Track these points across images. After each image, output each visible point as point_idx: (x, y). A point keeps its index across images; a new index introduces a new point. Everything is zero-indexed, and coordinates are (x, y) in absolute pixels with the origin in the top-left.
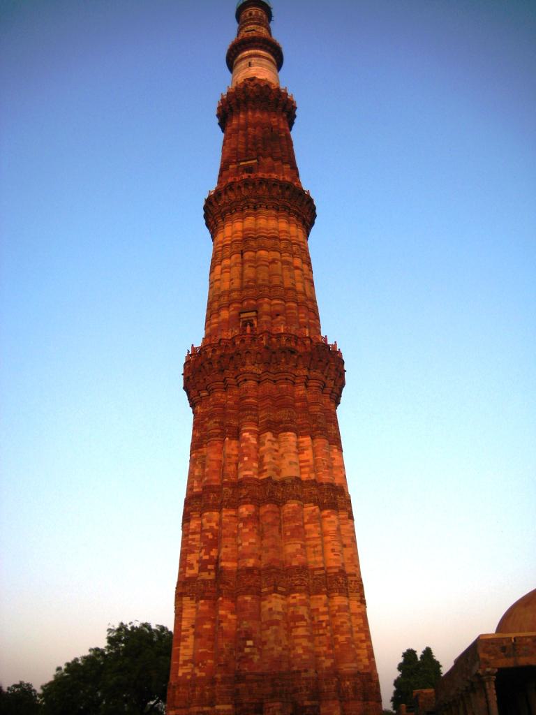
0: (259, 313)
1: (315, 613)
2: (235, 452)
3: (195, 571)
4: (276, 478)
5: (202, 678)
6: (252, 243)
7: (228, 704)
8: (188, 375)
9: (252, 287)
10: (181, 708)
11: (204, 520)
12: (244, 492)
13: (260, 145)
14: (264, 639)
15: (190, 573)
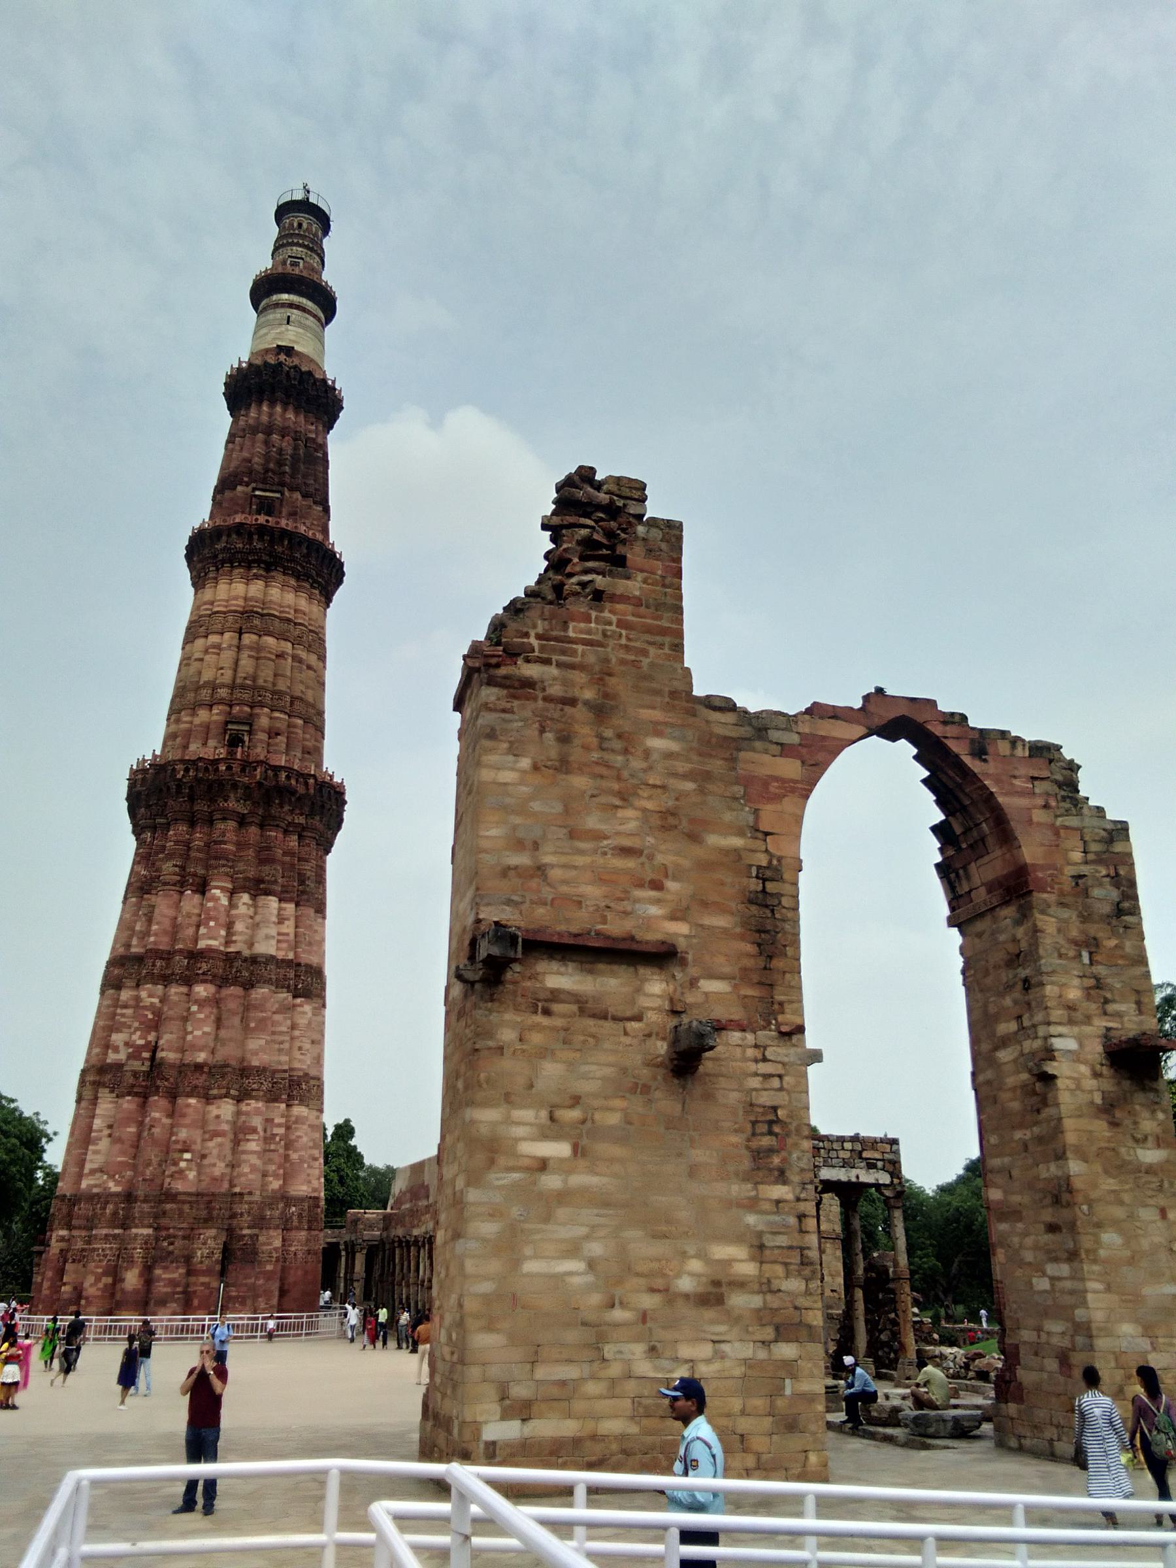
0: (255, 727)
1: (269, 1125)
2: (197, 911)
3: (122, 1056)
4: (246, 953)
5: (117, 1195)
6: (257, 622)
7: (149, 1226)
8: (139, 788)
9: (249, 686)
10: (80, 1228)
11: (144, 994)
12: (205, 967)
13: (287, 469)
14: (204, 1152)
15: (112, 1057)
